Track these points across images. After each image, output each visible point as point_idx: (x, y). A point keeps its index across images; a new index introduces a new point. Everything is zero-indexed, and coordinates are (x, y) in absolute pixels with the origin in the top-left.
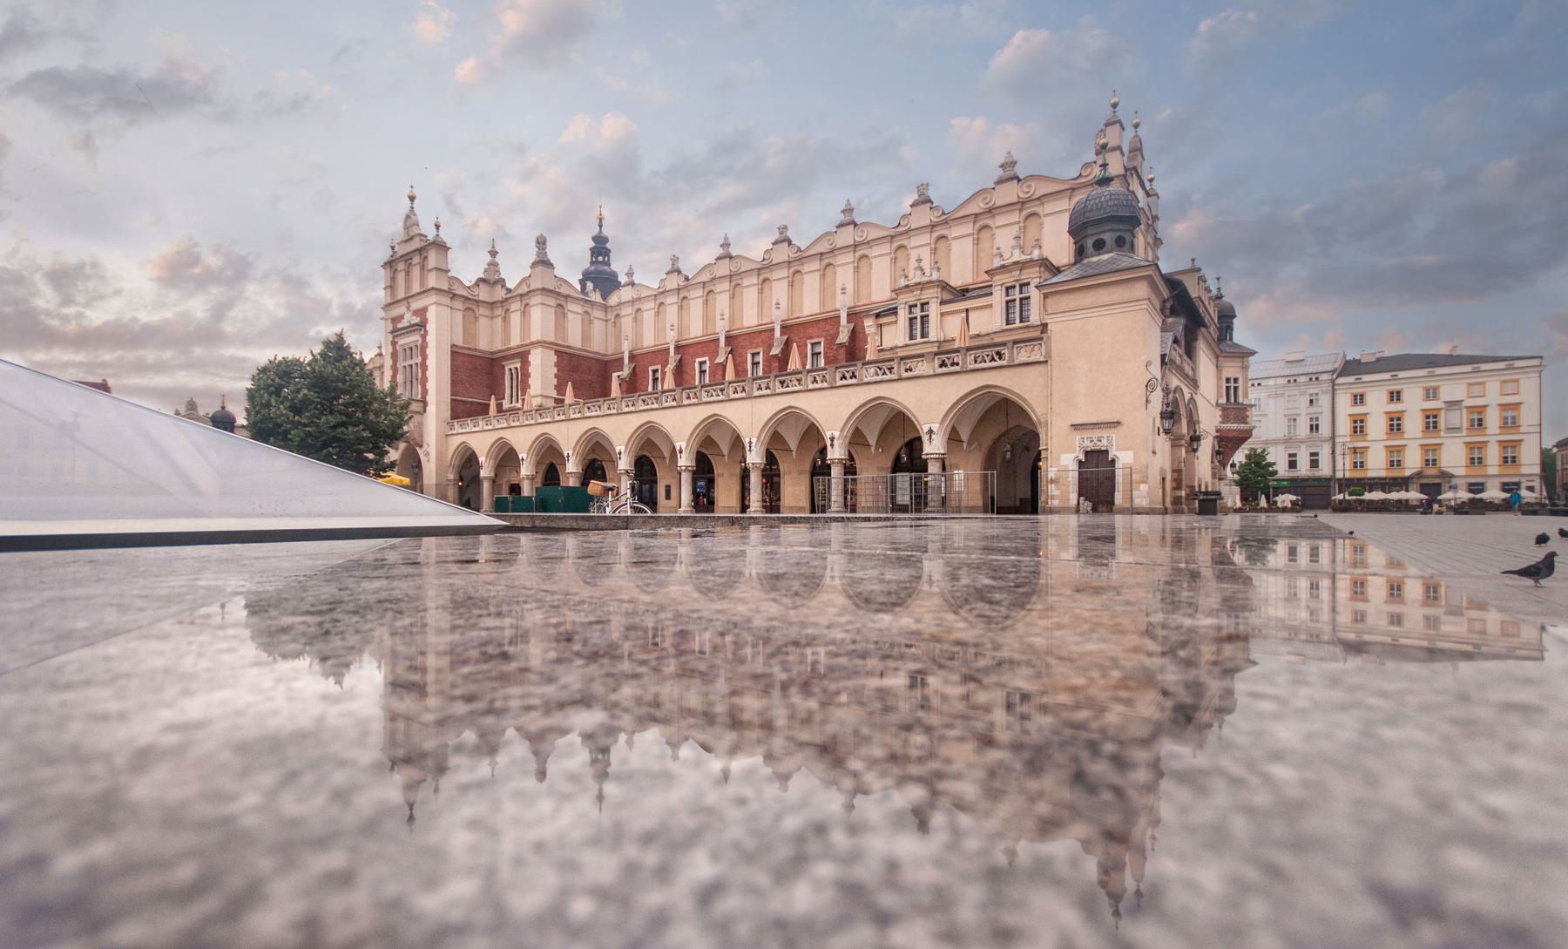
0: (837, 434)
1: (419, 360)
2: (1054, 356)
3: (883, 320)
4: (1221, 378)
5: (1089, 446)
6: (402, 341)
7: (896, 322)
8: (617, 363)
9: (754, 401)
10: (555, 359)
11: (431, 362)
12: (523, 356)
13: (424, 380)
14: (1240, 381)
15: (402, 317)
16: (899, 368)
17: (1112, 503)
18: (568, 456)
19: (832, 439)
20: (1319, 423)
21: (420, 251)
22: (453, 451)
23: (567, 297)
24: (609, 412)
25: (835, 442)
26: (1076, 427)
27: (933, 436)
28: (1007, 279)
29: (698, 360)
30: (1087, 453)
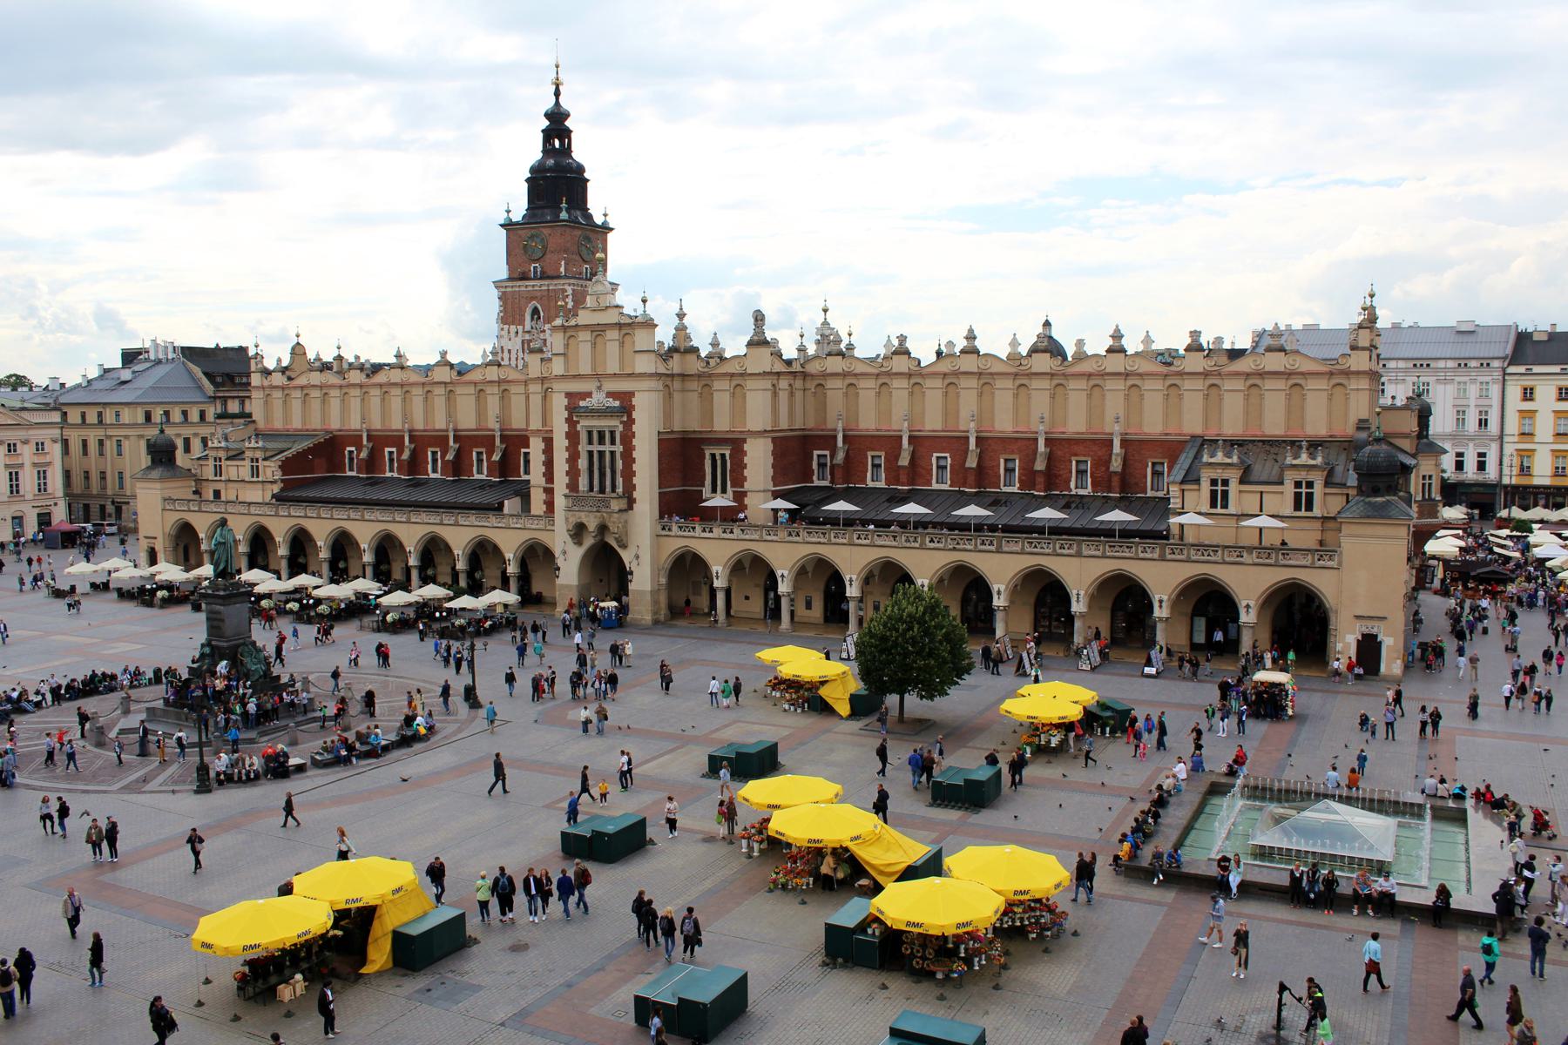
1: (618, 448)
2: (1344, 564)
5: (1366, 631)
6: (584, 424)
7: (1199, 490)
8: (828, 441)
9: (1083, 559)
10: (770, 447)
12: (736, 444)
13: (629, 474)
15: (589, 395)
16: (1223, 554)
17: (1379, 670)
18: (851, 580)
19: (1161, 602)
20: (1489, 418)
21: (620, 326)
22: (673, 549)
23: (778, 374)
24: (908, 545)
25: (1164, 604)
26: (1357, 617)
28: (1302, 476)
29: (935, 455)
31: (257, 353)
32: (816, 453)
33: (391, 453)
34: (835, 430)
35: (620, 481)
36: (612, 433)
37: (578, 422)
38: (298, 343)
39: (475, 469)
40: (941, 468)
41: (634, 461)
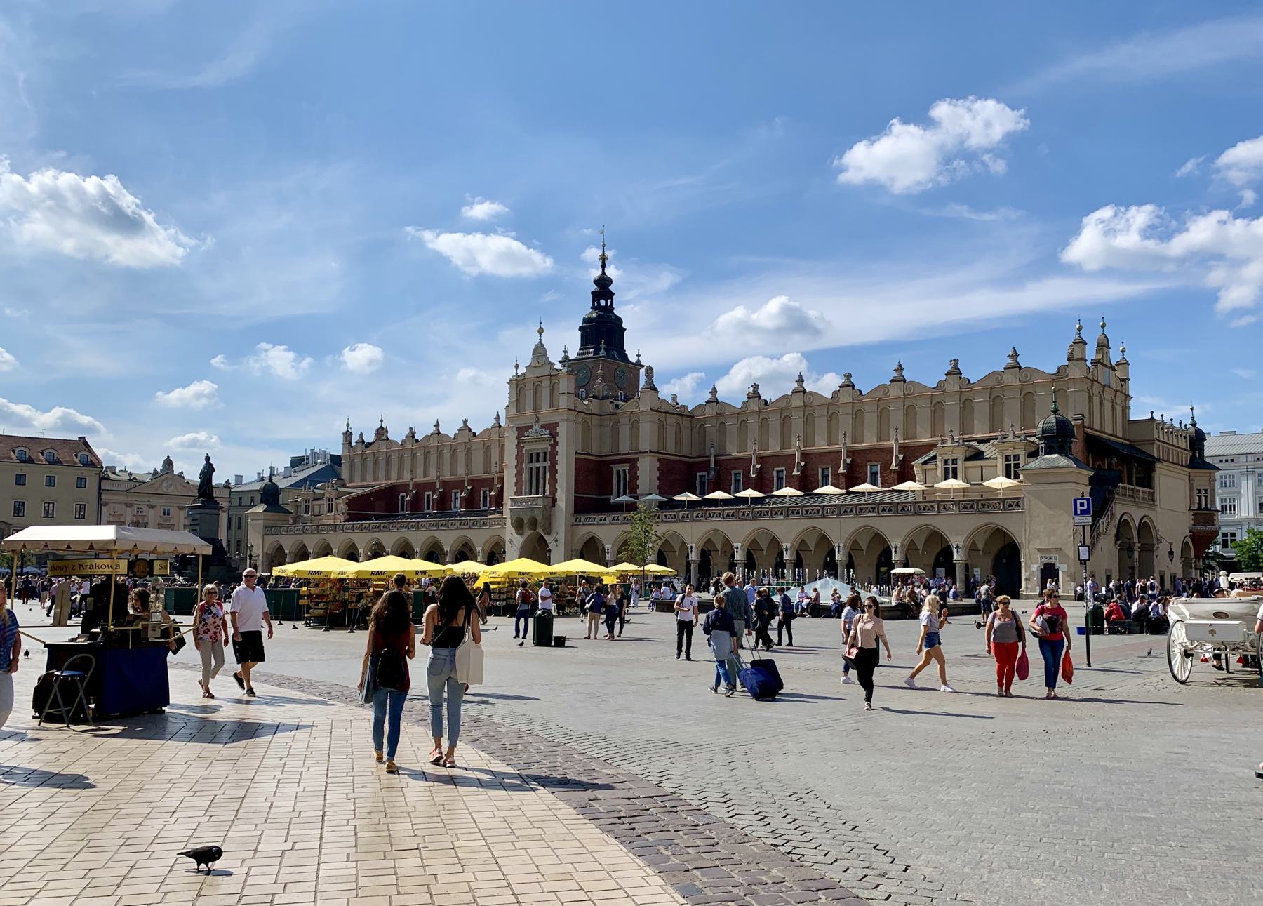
0: (899, 545)
1: (548, 464)
3: (926, 467)
4: (1193, 489)
8: (705, 466)
11: (561, 468)
12: (633, 463)
13: (554, 480)
14: (1209, 492)
15: (531, 427)
18: (691, 548)
23: (666, 413)
25: (898, 549)
27: (959, 550)
29: (775, 469)
30: (1045, 565)
31: (348, 431)
32: (698, 474)
33: (428, 496)
34: (709, 456)
35: (548, 486)
36: (545, 453)
37: (523, 447)
38: (381, 427)
39: (481, 503)
40: (780, 479)
41: (556, 471)
